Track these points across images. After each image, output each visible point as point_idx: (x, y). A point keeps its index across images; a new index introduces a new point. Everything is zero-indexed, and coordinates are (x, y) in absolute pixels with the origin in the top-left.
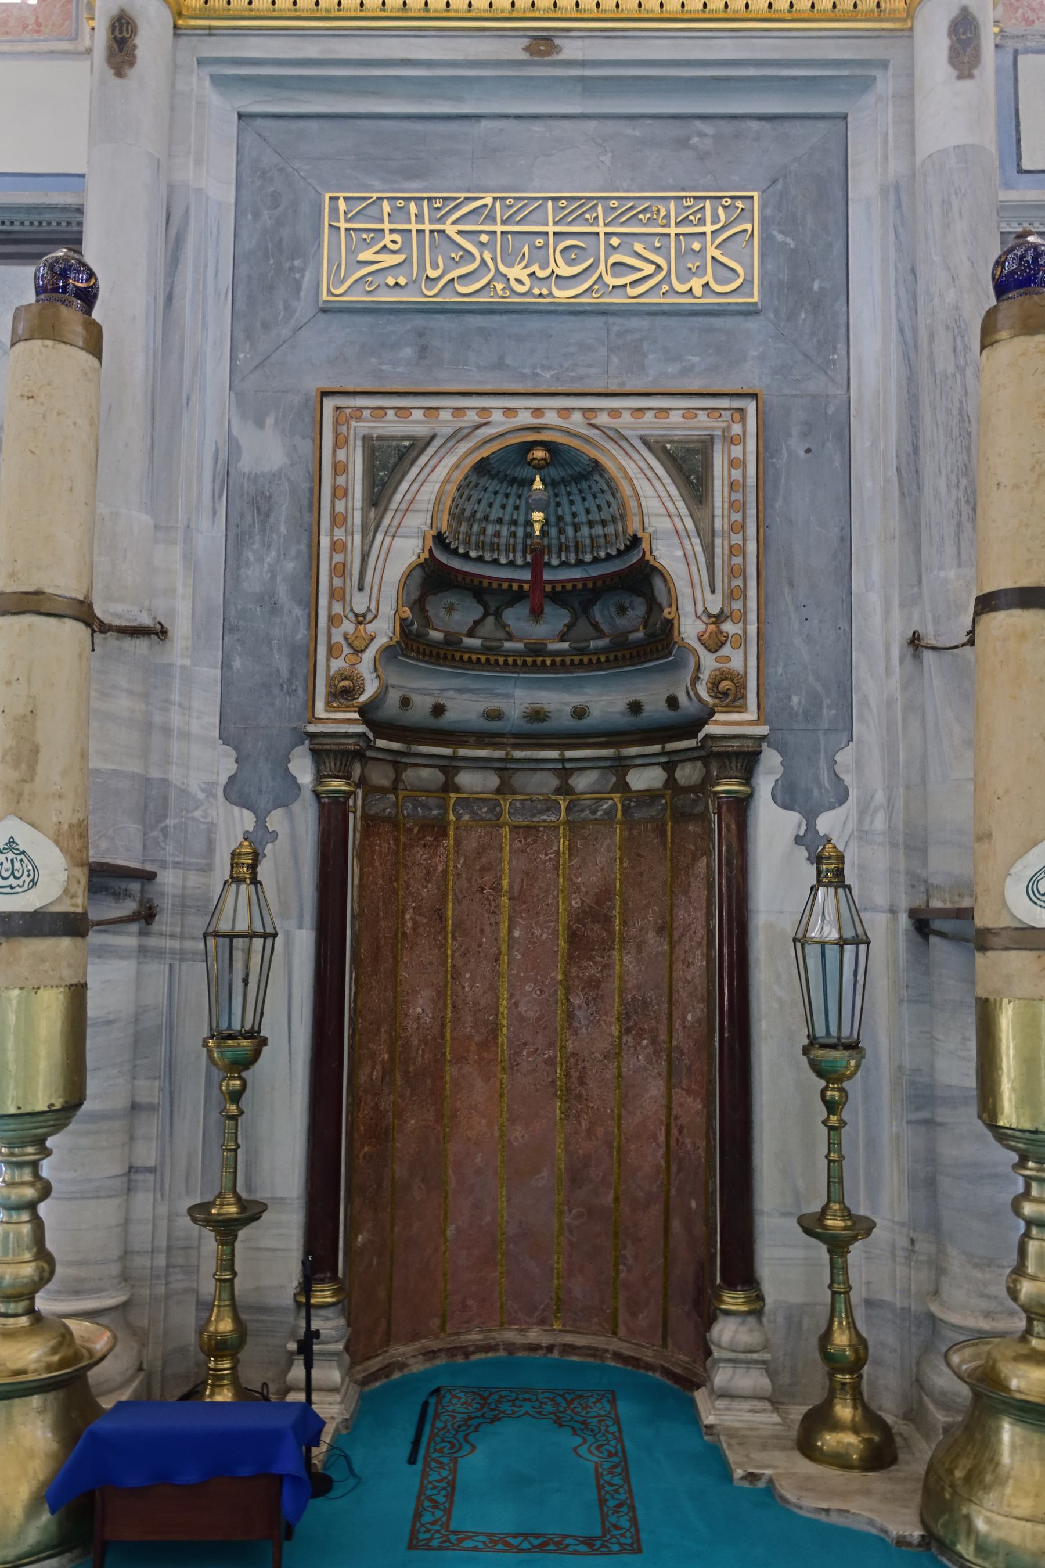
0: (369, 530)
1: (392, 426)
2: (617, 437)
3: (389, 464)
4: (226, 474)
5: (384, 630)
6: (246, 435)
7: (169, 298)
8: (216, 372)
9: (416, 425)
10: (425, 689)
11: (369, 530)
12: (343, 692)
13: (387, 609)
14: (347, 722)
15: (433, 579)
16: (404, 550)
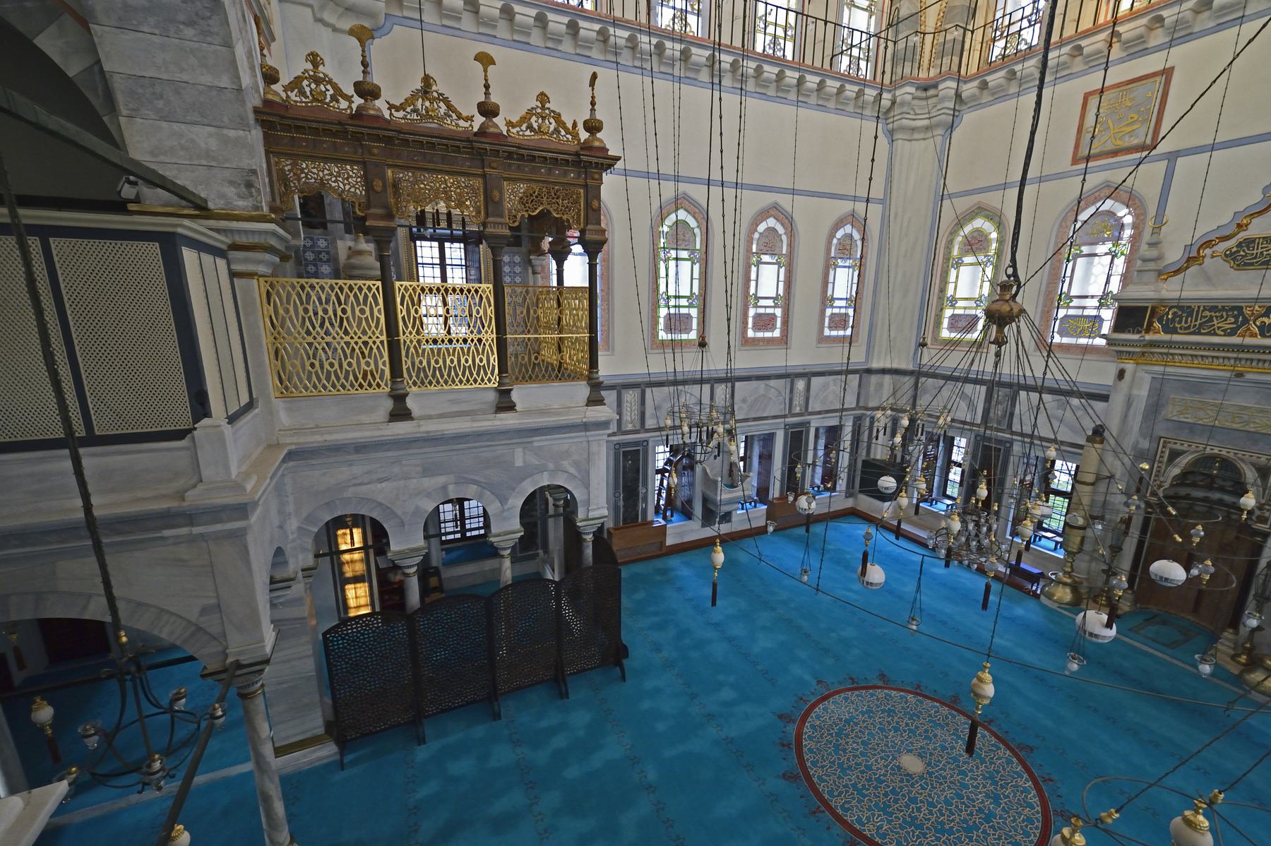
0: (1167, 466)
1: (1178, 447)
2: (1242, 460)
3: (1174, 455)
4: (1135, 447)
5: (1167, 485)
6: (1141, 440)
7: (1126, 416)
8: (1136, 428)
9: (1185, 447)
10: (1183, 491)
11: (1167, 466)
12: (1154, 494)
13: (1169, 481)
14: (1154, 500)
15: (1184, 474)
16: (1176, 471)
